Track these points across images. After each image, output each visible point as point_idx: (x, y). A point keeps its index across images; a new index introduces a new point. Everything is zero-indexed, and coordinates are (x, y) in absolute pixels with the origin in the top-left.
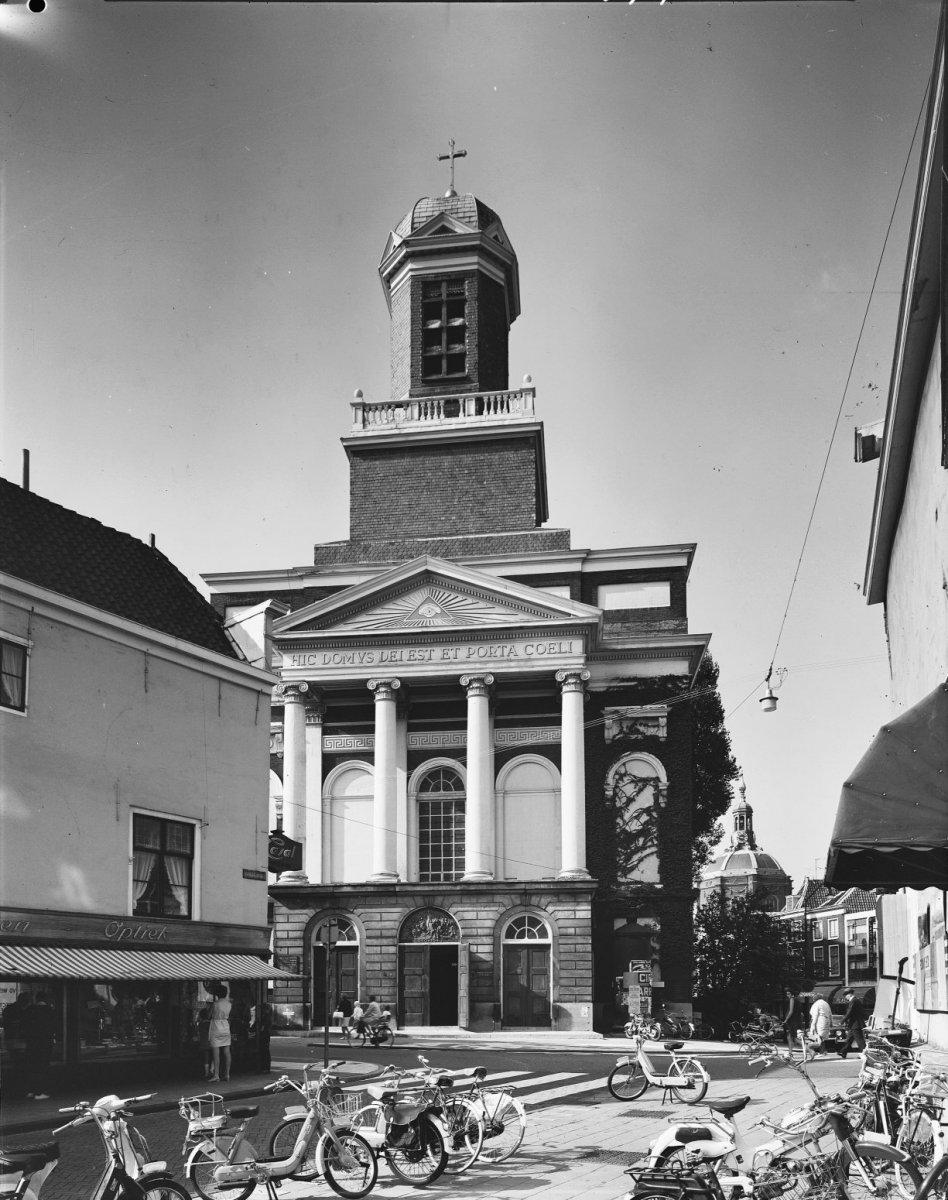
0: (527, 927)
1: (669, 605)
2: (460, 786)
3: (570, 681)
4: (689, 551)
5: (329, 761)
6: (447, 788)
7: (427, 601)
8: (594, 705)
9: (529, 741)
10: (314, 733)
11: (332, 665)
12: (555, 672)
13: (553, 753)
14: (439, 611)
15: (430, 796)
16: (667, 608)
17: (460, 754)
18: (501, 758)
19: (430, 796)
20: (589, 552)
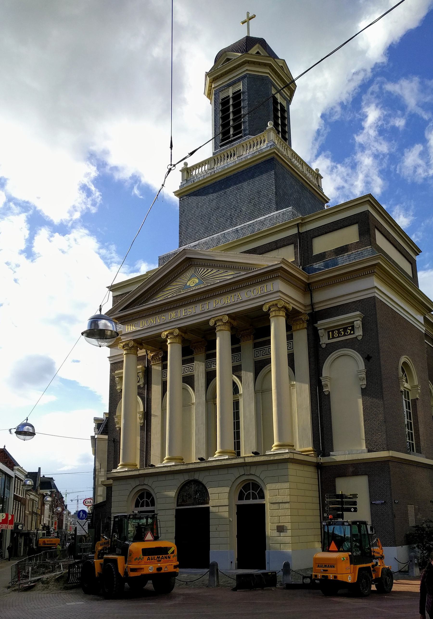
0: (251, 491)
12: (262, 305)
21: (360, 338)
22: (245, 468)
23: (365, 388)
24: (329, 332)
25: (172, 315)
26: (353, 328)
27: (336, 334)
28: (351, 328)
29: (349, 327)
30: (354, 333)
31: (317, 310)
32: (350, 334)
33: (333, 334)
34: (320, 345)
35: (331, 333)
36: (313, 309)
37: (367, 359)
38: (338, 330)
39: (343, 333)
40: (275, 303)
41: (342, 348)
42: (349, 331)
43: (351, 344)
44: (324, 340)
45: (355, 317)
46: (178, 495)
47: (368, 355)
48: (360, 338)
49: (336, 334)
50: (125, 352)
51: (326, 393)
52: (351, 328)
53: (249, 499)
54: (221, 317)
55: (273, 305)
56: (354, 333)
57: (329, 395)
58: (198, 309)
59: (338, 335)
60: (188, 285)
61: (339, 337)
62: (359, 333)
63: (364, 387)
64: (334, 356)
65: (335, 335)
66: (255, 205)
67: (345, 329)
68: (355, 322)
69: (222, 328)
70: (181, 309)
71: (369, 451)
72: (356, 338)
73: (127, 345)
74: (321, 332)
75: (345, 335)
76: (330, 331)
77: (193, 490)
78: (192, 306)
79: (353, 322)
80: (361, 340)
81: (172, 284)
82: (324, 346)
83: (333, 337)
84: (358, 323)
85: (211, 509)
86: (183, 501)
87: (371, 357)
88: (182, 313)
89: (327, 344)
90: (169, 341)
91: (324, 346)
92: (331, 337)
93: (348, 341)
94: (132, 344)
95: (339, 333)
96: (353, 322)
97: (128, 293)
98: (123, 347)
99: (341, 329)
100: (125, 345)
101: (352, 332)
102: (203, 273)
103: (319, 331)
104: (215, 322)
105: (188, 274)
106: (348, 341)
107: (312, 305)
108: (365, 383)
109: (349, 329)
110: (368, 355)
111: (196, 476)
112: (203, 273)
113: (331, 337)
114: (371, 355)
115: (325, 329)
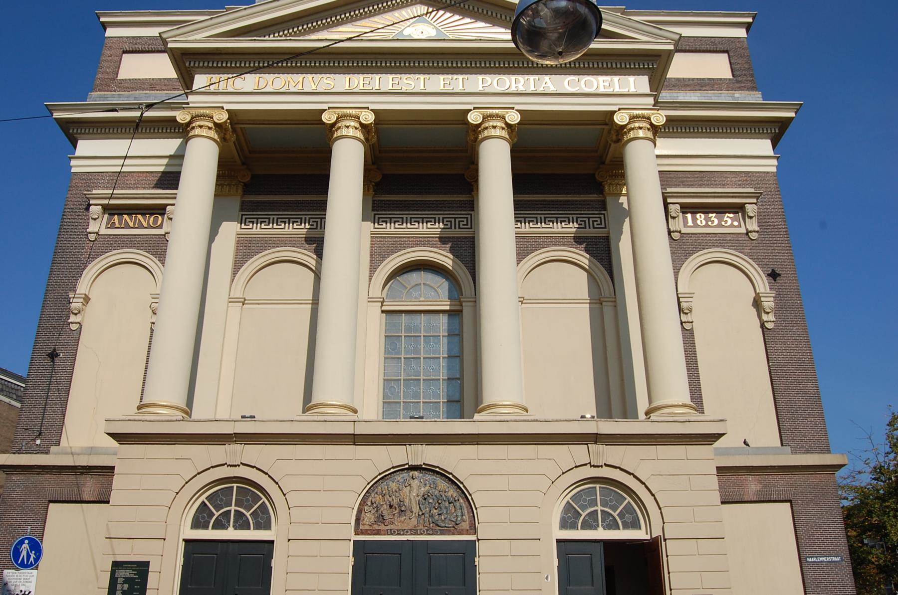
0: (599, 508)
12: (613, 112)
16: (730, 80)
25: (359, 81)
32: (732, 226)
33: (694, 220)
37: (773, 275)
42: (729, 222)
46: (363, 503)
47: (773, 270)
48: (754, 236)
53: (596, 528)
58: (439, 82)
59: (707, 222)
61: (707, 226)
70: (384, 76)
85: (482, 548)
86: (381, 518)
88: (387, 81)
92: (690, 223)
93: (729, 238)
99: (712, 213)
101: (736, 223)
106: (729, 238)
110: (773, 270)
113: (690, 223)
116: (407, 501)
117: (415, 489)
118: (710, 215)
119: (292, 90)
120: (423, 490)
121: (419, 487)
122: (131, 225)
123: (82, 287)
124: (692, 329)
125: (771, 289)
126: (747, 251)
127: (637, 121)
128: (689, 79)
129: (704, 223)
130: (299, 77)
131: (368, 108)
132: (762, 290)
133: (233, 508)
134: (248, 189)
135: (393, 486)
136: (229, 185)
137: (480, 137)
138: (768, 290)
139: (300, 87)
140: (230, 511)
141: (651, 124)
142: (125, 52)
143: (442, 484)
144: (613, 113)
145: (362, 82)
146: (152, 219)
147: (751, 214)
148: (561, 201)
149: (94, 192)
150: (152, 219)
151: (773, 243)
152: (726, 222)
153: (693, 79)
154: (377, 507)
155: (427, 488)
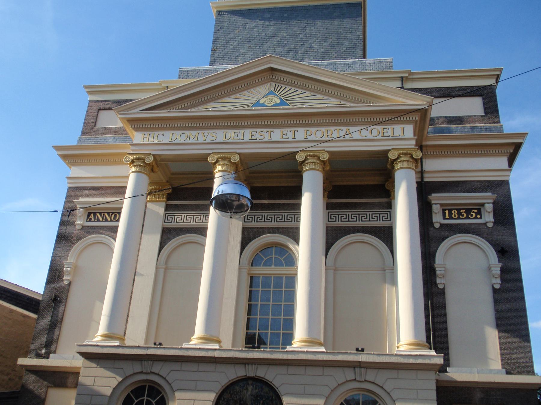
1: (483, 114)
2: (291, 261)
3: (402, 159)
4: (501, 70)
5: (167, 236)
6: (278, 264)
7: (270, 93)
8: (424, 190)
9: (359, 224)
10: (158, 209)
11: (178, 141)
12: (388, 151)
13: (387, 236)
14: (278, 101)
15: (260, 270)
16: (482, 116)
17: (293, 234)
18: (332, 236)
19: (260, 270)
20: (410, 73)
21: (490, 225)
22: (357, 370)
23: (499, 289)
24: (444, 210)
26: (479, 212)
27: (455, 214)
28: (476, 211)
29: (475, 209)
30: (481, 218)
31: (426, 180)
32: (476, 218)
34: (432, 223)
35: (447, 212)
36: (422, 177)
38: (459, 210)
39: (465, 215)
40: (409, 151)
41: (465, 233)
42: (474, 214)
43: (478, 230)
44: (438, 219)
45: (487, 199)
48: (490, 225)
49: (455, 214)
50: (133, 169)
51: (441, 287)
52: (476, 211)
54: (316, 153)
55: (407, 153)
56: (481, 218)
57: (443, 290)
60: (261, 102)
61: (459, 218)
62: (488, 218)
63: (497, 287)
64: (453, 240)
65: (453, 216)
66: (331, 45)
67: (468, 211)
68: (486, 205)
69: (313, 166)
71: (508, 373)
72: (485, 224)
73: (142, 160)
74: (436, 208)
75: (467, 218)
76: (447, 210)
77: (249, 393)
78: (265, 130)
79: (483, 205)
80: (492, 228)
81: (233, 96)
82: (437, 226)
83: (451, 218)
84: (489, 207)
87: (506, 252)
88: (246, 134)
89: (441, 225)
90: (219, 168)
91: (437, 226)
92: (447, 217)
93: (473, 226)
94: (150, 160)
95: (459, 213)
96: (483, 205)
97: (131, 100)
98: (133, 162)
99: (463, 209)
100: (139, 159)
101: (478, 216)
102: (288, 93)
103: (434, 207)
104: (306, 157)
105: (263, 90)
106: (473, 226)
107: (422, 173)
108: (500, 282)
109: (474, 212)
111: (261, 372)
112: (288, 93)
113: (447, 217)
114: (506, 249)
115: (442, 205)
116: (245, 398)
117: (250, 391)
118: (462, 211)
119: (192, 141)
120: (255, 391)
121: (252, 389)
122: (101, 219)
123: (71, 259)
124: (444, 288)
125: (499, 262)
126: (485, 235)
127: (402, 157)
128: (453, 117)
129: (457, 216)
130: (194, 133)
131: (236, 152)
132: (493, 263)
133: (145, 398)
134: (170, 197)
135: (237, 388)
136: (159, 195)
137: (304, 169)
138: (497, 262)
139: (196, 139)
140: (144, 400)
141: (412, 157)
142: (100, 109)
143: (266, 389)
144: (388, 151)
145: (233, 135)
146: (113, 216)
147: (489, 210)
148: (362, 203)
149: (81, 200)
150: (113, 216)
151: (504, 230)
152: (472, 215)
153: (456, 117)
154: (227, 401)
155: (257, 390)
